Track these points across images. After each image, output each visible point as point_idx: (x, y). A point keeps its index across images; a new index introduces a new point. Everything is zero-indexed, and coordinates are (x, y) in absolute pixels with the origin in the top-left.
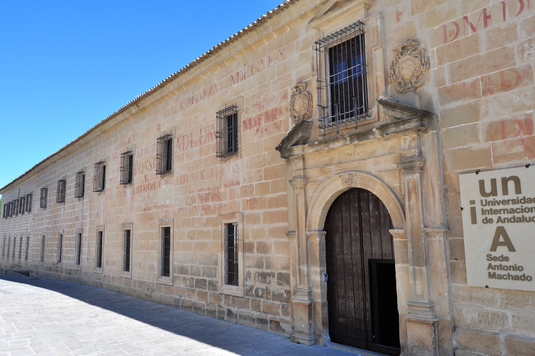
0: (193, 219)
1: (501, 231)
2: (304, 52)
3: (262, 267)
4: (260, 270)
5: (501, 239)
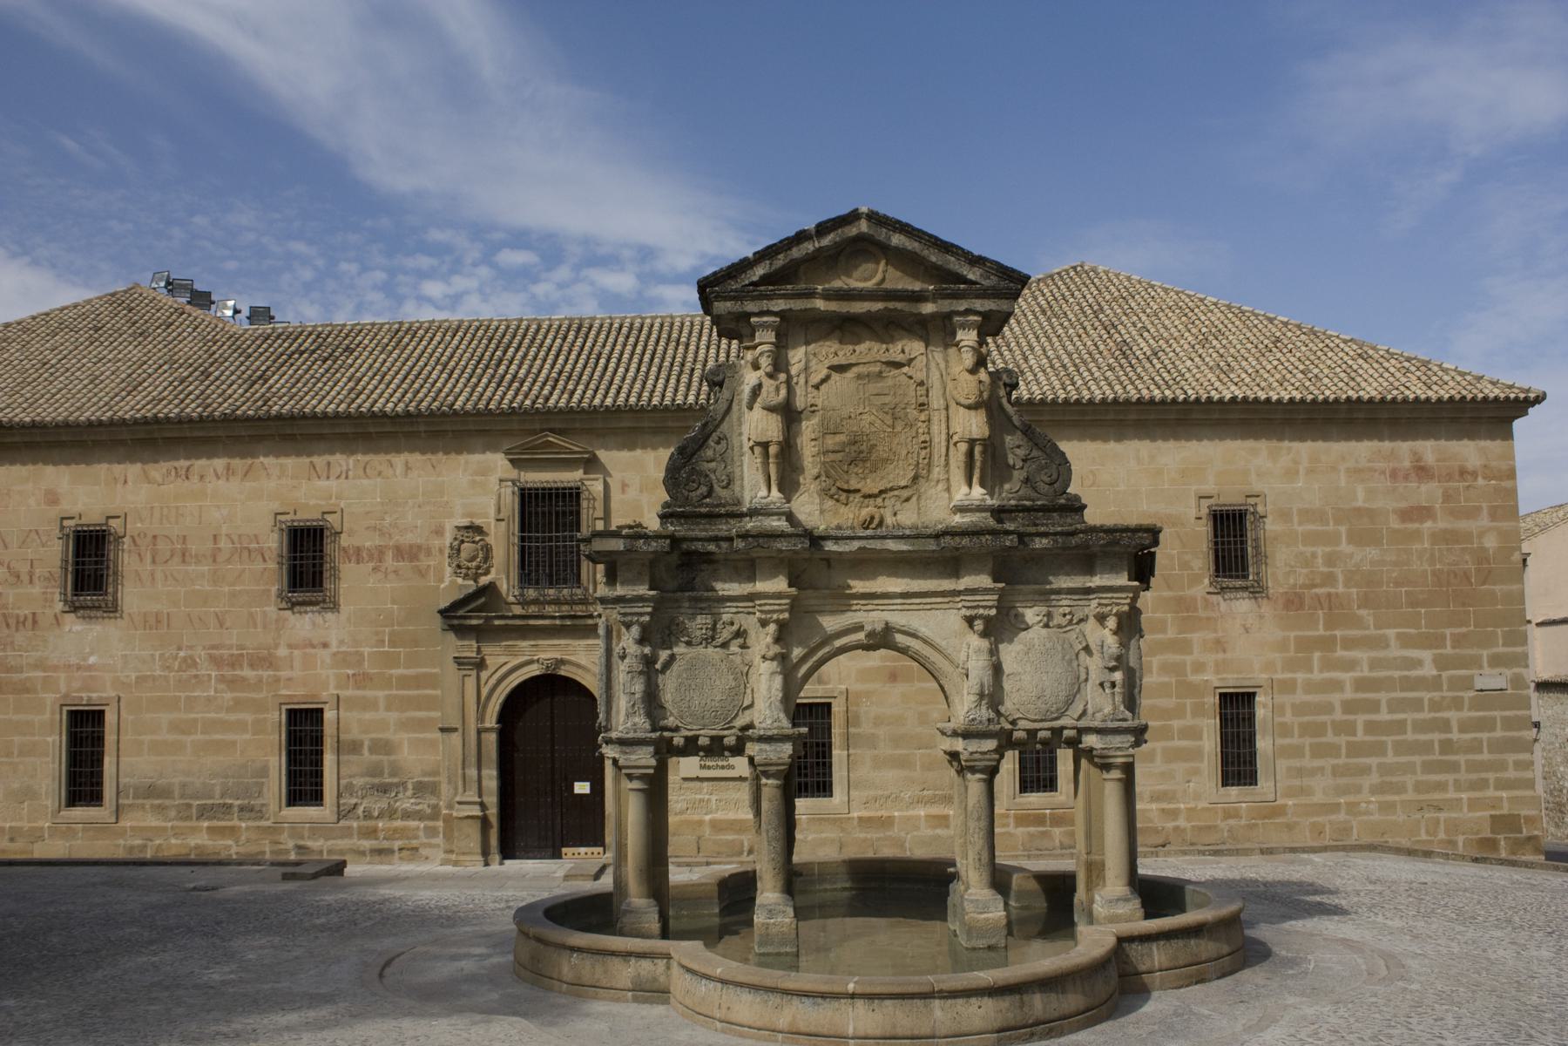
0: (188, 698)
2: (478, 478)
3: (381, 774)
4: (376, 781)
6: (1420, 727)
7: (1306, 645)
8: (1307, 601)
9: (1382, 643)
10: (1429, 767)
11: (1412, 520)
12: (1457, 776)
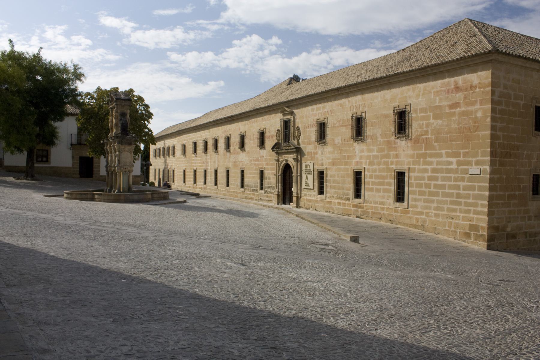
1: (307, 176)
5: (307, 178)
6: (450, 187)
7: (419, 156)
8: (420, 140)
9: (440, 155)
10: (452, 203)
11: (453, 108)
12: (461, 207)
